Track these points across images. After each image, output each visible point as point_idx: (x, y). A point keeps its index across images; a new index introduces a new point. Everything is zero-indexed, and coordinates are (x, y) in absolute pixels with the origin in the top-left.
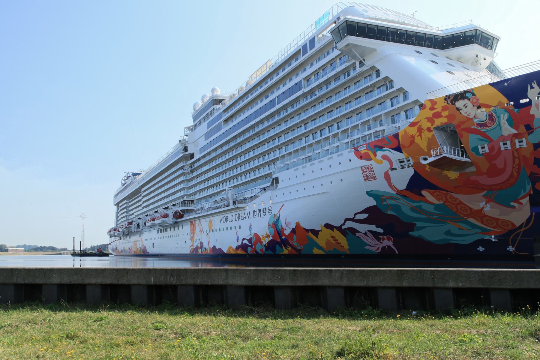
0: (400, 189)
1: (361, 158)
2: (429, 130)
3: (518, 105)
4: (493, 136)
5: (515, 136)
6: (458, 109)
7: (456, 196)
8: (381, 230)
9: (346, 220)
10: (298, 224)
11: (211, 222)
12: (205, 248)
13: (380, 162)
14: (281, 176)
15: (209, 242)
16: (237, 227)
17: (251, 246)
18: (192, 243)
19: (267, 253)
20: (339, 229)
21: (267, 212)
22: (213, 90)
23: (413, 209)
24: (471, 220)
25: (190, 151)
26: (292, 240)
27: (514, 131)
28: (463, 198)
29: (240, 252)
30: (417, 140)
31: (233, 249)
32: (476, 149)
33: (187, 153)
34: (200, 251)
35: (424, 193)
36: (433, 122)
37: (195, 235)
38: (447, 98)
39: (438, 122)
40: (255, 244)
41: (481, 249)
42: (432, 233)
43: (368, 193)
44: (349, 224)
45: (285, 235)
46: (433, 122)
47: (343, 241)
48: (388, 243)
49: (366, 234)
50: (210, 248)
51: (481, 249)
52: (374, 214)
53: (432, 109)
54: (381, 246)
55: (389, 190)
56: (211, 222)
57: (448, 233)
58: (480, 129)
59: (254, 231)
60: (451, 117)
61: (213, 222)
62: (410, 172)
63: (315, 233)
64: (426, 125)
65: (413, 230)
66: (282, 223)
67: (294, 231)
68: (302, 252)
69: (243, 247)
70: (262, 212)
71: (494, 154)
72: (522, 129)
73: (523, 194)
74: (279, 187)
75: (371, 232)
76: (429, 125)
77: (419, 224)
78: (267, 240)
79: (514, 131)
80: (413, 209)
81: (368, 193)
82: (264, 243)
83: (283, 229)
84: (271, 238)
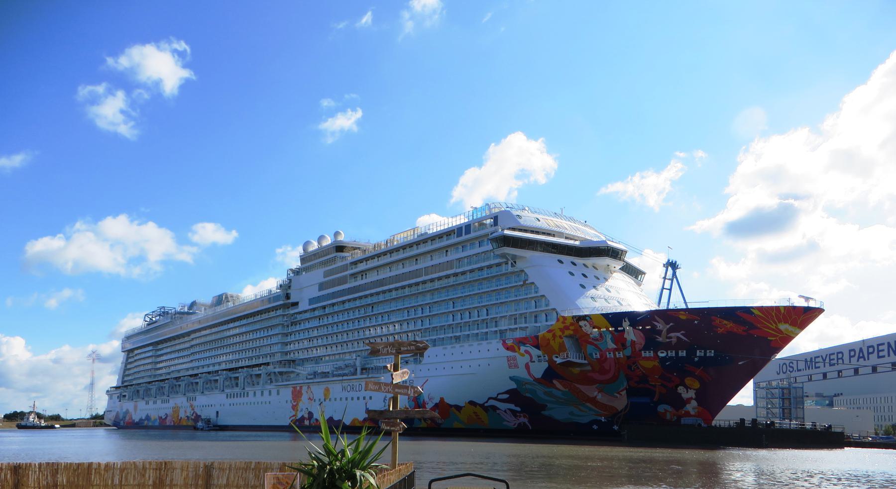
2: (560, 337)
3: (616, 330)
4: (603, 347)
5: (615, 350)
6: (581, 327)
8: (518, 409)
9: (489, 399)
10: (442, 400)
11: (327, 390)
12: (317, 420)
13: (523, 355)
16: (367, 398)
18: (293, 413)
20: (482, 406)
23: (545, 393)
24: (588, 404)
25: (292, 300)
27: (615, 347)
28: (582, 388)
30: (552, 342)
31: (359, 422)
32: (591, 355)
33: (290, 301)
34: (307, 423)
35: (555, 382)
36: (563, 333)
37: (300, 404)
38: (574, 317)
39: (567, 332)
41: (595, 427)
42: (559, 413)
43: (511, 378)
44: (492, 402)
46: (563, 333)
48: (523, 420)
49: (505, 411)
51: (595, 427)
52: (514, 396)
53: (563, 323)
54: (517, 422)
55: (528, 377)
56: (327, 390)
58: (595, 342)
60: (576, 328)
61: (331, 390)
62: (545, 365)
63: (458, 408)
64: (559, 333)
67: (436, 406)
68: (442, 426)
71: (603, 360)
76: (560, 333)
77: (549, 405)
79: (615, 347)
80: (545, 393)
81: (511, 378)
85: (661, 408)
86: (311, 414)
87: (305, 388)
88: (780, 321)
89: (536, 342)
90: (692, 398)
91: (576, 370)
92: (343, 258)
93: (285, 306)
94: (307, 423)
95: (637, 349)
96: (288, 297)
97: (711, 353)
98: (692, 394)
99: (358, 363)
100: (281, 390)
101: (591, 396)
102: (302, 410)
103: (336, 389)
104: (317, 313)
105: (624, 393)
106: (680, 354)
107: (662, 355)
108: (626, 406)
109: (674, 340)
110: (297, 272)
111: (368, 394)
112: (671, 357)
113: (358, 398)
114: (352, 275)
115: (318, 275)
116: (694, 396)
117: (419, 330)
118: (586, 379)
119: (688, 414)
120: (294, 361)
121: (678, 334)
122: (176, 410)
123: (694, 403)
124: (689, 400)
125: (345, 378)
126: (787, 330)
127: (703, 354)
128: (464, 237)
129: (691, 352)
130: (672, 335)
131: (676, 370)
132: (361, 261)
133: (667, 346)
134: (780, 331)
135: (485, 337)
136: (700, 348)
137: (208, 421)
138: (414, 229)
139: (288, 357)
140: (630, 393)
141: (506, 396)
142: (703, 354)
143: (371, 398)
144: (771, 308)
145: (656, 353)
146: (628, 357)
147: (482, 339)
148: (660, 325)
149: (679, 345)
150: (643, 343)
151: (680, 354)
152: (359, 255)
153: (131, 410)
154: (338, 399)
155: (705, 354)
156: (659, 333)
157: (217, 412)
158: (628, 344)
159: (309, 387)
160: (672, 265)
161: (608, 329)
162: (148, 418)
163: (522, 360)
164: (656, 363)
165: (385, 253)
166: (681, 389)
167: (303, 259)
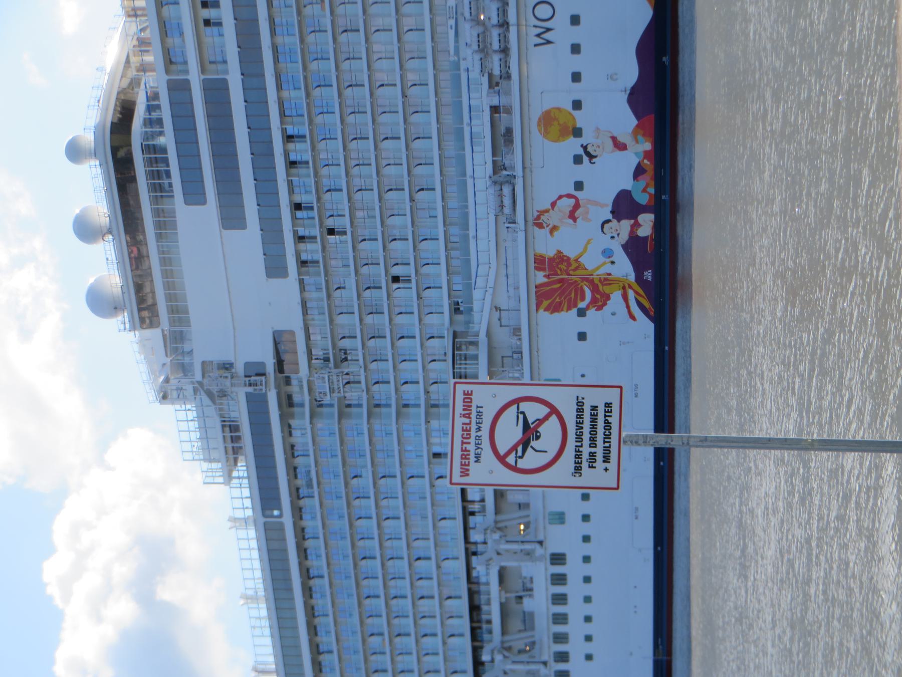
18: (616, 297)
50: (635, 133)
92: (153, 97)
94: (646, 224)
96: (255, 371)
103: (544, 77)
115: (196, 224)
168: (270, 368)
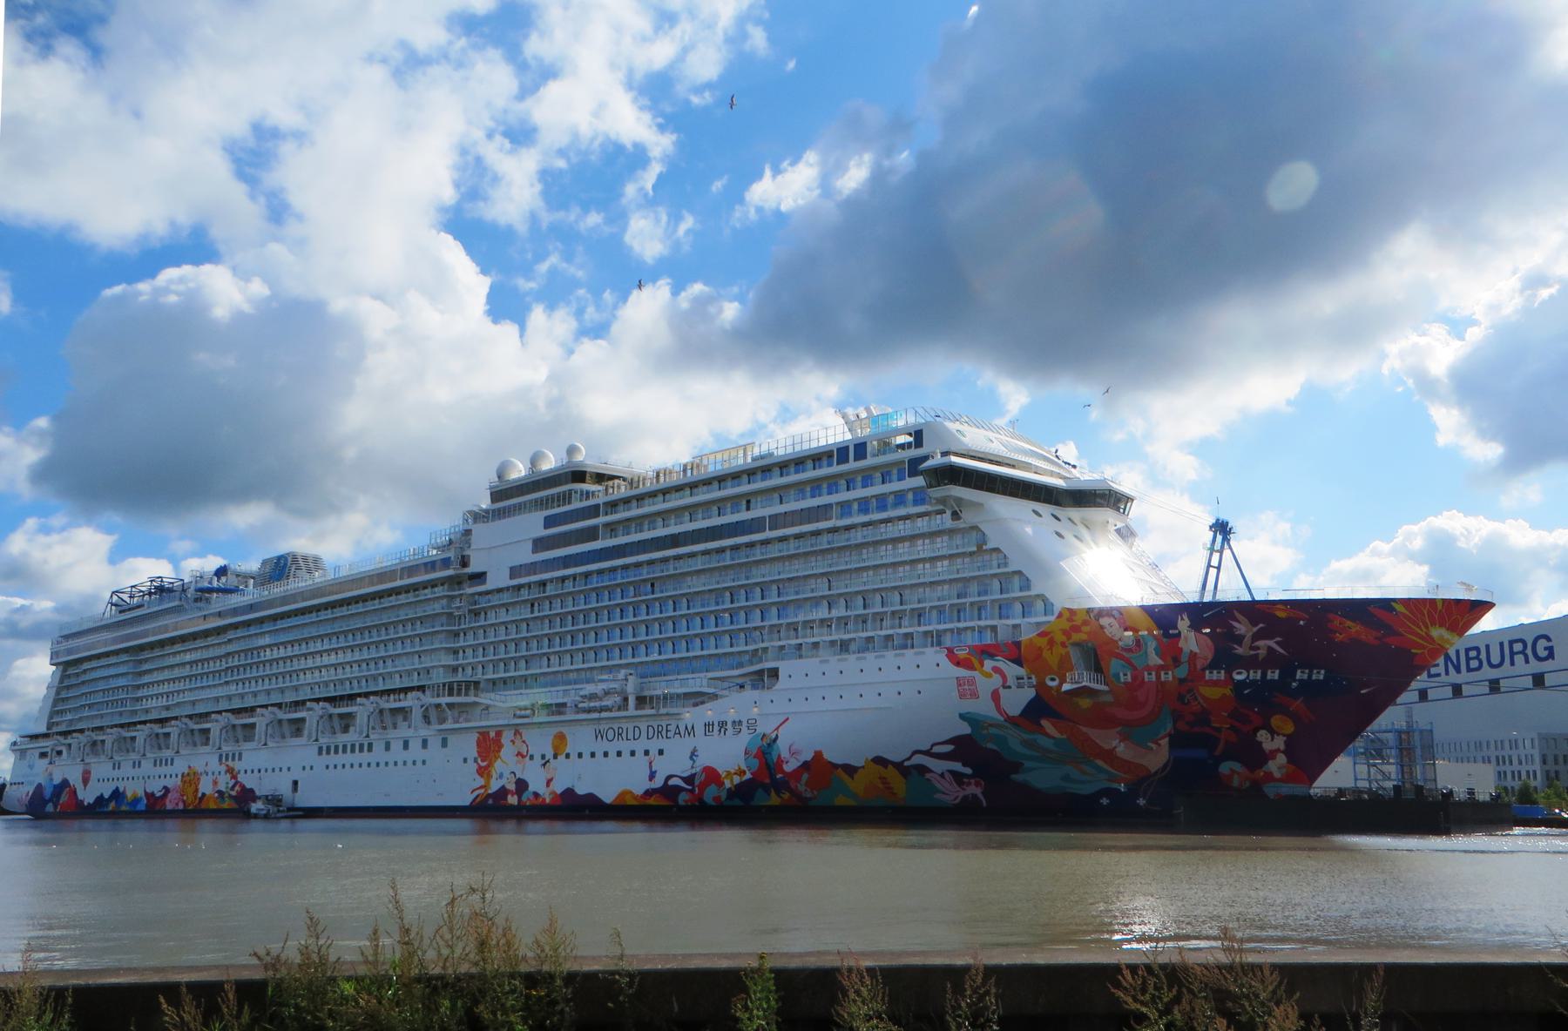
0: (1011, 713)
1: (958, 664)
3: (1166, 634)
4: (1138, 663)
5: (1159, 668)
6: (1102, 627)
7: (1084, 729)
8: (968, 771)
11: (561, 738)
12: (536, 795)
13: (988, 676)
14: (784, 667)
15: (549, 782)
16: (654, 752)
17: (692, 791)
18: (481, 781)
19: (729, 803)
20: (898, 766)
21: (744, 728)
22: (572, 450)
23: (1025, 743)
24: (1100, 763)
26: (798, 779)
27: (1160, 662)
28: (1094, 734)
29: (652, 801)
30: (1046, 654)
31: (635, 797)
35: (1044, 723)
37: (498, 764)
39: (1076, 637)
40: (703, 786)
41: (1105, 801)
42: (1042, 777)
43: (962, 716)
44: (919, 759)
45: (783, 772)
46: (1069, 638)
47: (899, 784)
48: (974, 790)
49: (942, 775)
50: (553, 793)
51: (1105, 801)
52: (963, 747)
53: (1070, 620)
54: (961, 794)
57: (1066, 778)
59: (704, 760)
62: (1030, 693)
63: (850, 770)
65: (1017, 772)
66: (782, 747)
69: (668, 791)
70: (729, 726)
71: (1138, 682)
72: (1170, 662)
73: (1163, 733)
74: (777, 687)
75: (952, 772)
76: (1064, 638)
77: (1028, 764)
78: (737, 780)
79: (1160, 662)
80: (1025, 743)
81: (962, 716)
82: (728, 784)
83: (780, 761)
84: (748, 776)
85: (1225, 768)
86: (522, 785)
87: (506, 738)
88: (1433, 624)
89: (1015, 653)
90: (1278, 750)
91: (1085, 703)
93: (456, 581)
94: (512, 800)
95: (1199, 667)
96: (464, 562)
97: (1319, 675)
98: (1279, 743)
99: (630, 688)
100: (451, 739)
101: (1106, 747)
102: (501, 776)
104: (525, 595)
105: (1164, 742)
106: (1269, 676)
107: (1239, 677)
108: (1165, 766)
109: (1262, 653)
110: (479, 517)
111: (654, 746)
112: (1254, 682)
113: (633, 753)
114: (607, 525)
115: (532, 524)
116: (1282, 747)
117: (755, 628)
118: (1102, 718)
119: (1269, 777)
120: (477, 683)
121: (1271, 643)
122: (191, 779)
123: (1282, 759)
124: (1273, 754)
125: (604, 715)
126: (1442, 637)
127: (1305, 677)
128: (852, 465)
129: (1288, 673)
130: (1261, 643)
131: (1257, 703)
132: (626, 501)
133: (1249, 663)
134: (1430, 639)
135: (907, 641)
136: (1302, 666)
137: (274, 800)
138: (745, 448)
139: (460, 677)
140: (1176, 741)
141: (949, 748)
142: (1305, 677)
143: (661, 752)
144: (1424, 601)
145: (1229, 673)
146: (1181, 681)
147: (905, 647)
148: (1242, 627)
149: (1272, 659)
150: (1210, 656)
151: (1269, 676)
152: (623, 491)
153: (75, 779)
154: (586, 755)
155: (1310, 676)
156: (1239, 640)
157: (295, 783)
158: (1184, 658)
159: (517, 733)
160: (1222, 529)
161: (1150, 632)
162: (117, 795)
163: (985, 683)
164: (1228, 691)
165: (679, 488)
166: (1262, 735)
167: (497, 495)
168: (468, 570)
